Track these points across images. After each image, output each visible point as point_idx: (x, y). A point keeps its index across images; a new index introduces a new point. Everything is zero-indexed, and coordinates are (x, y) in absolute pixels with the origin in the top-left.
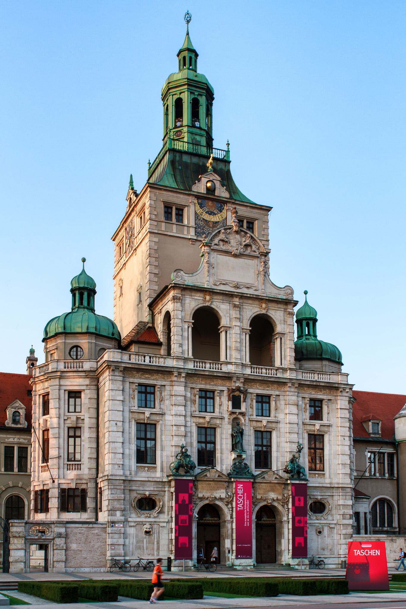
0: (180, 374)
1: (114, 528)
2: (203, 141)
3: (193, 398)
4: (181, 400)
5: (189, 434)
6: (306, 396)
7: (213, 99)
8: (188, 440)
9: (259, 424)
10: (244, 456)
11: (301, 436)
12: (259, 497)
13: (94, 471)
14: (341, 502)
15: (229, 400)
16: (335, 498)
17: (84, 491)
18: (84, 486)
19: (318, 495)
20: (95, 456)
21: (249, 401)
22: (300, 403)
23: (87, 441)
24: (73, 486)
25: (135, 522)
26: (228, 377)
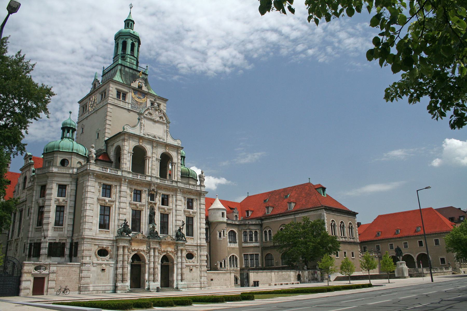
0: (125, 180)
2: (135, 63)
3: (130, 193)
6: (185, 196)
7: (140, 44)
13: (71, 233)
15: (148, 196)
16: (199, 251)
17: (64, 244)
18: (64, 241)
19: (191, 249)
20: (72, 223)
21: (158, 196)
23: (68, 214)
24: (57, 241)
25: (96, 264)
26: (149, 184)
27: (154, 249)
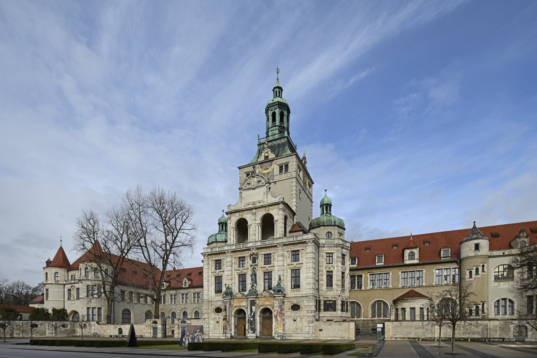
2: (277, 132)
4: (230, 263)
8: (233, 281)
9: (265, 269)
10: (255, 285)
11: (285, 272)
12: (261, 304)
14: (307, 304)
16: (305, 302)
22: (286, 254)
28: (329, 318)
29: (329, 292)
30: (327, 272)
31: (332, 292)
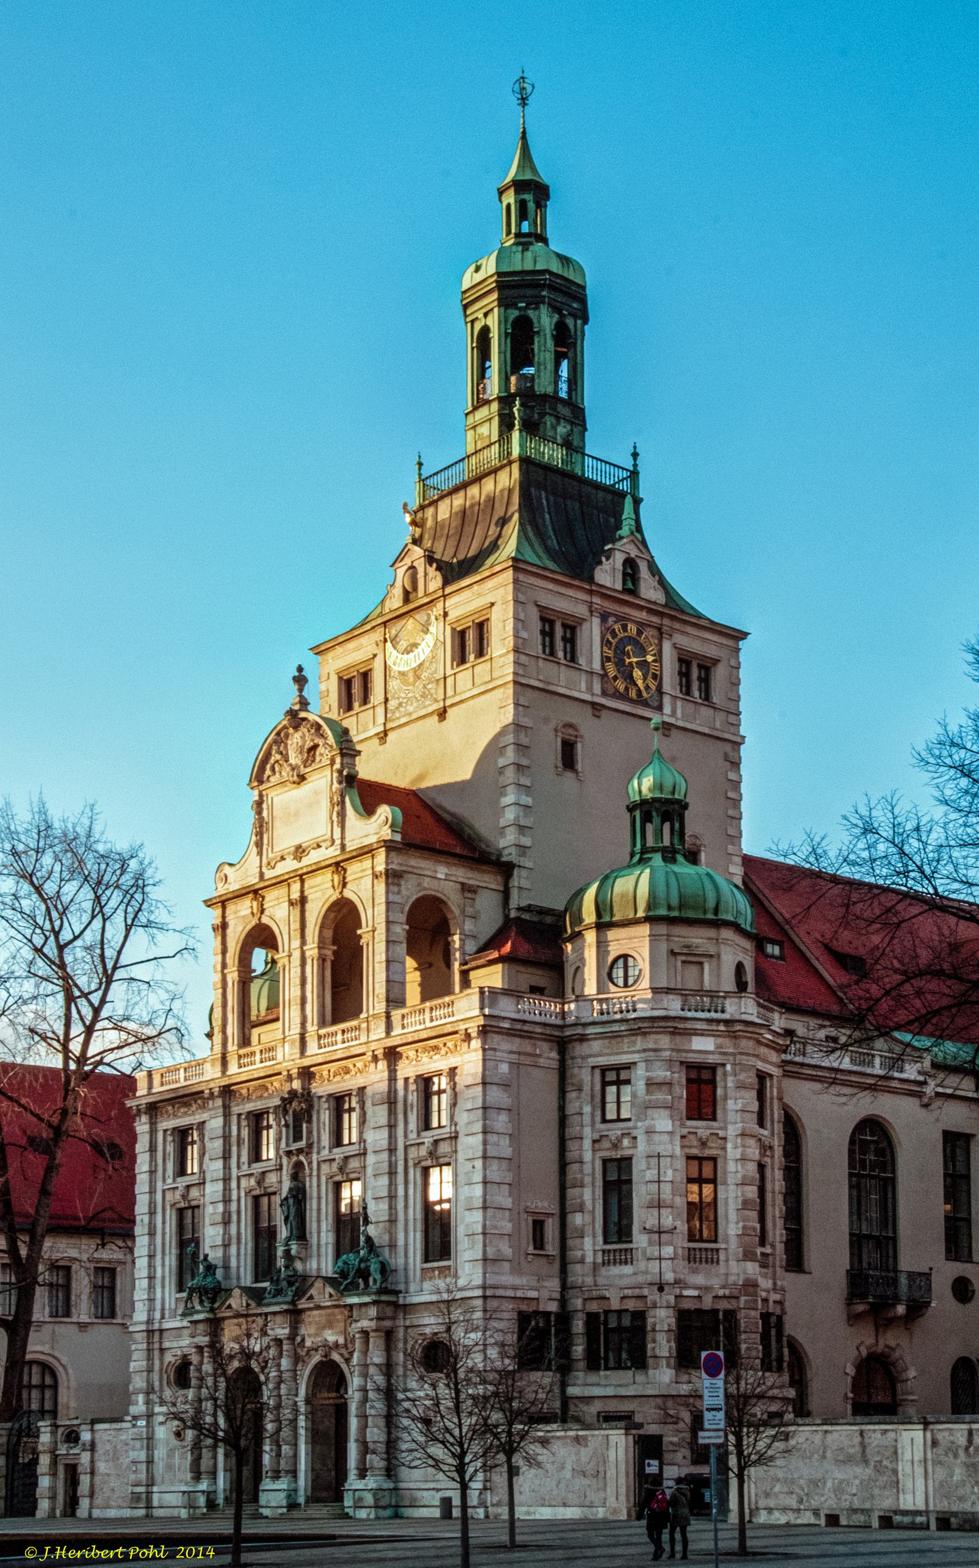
1: (135, 1430)
5: (234, 1217)
27: (279, 1342)
28: (613, 1406)
29: (615, 1270)
30: (605, 1162)
31: (627, 1269)
